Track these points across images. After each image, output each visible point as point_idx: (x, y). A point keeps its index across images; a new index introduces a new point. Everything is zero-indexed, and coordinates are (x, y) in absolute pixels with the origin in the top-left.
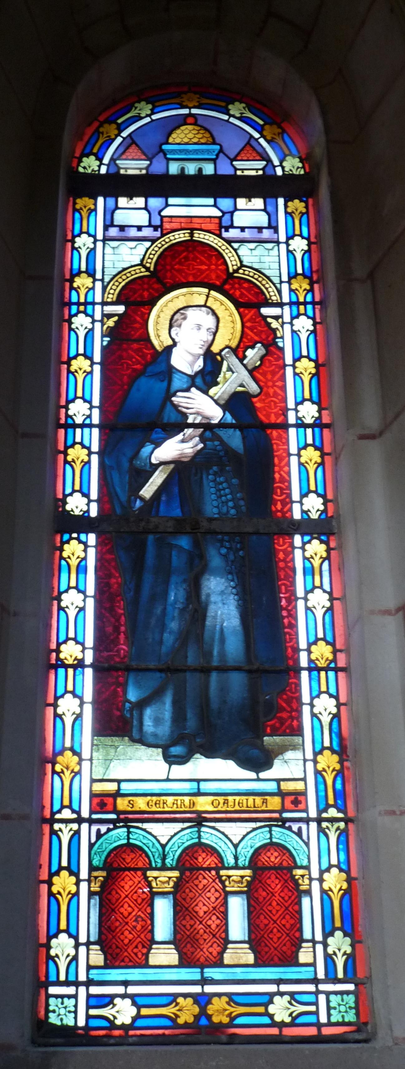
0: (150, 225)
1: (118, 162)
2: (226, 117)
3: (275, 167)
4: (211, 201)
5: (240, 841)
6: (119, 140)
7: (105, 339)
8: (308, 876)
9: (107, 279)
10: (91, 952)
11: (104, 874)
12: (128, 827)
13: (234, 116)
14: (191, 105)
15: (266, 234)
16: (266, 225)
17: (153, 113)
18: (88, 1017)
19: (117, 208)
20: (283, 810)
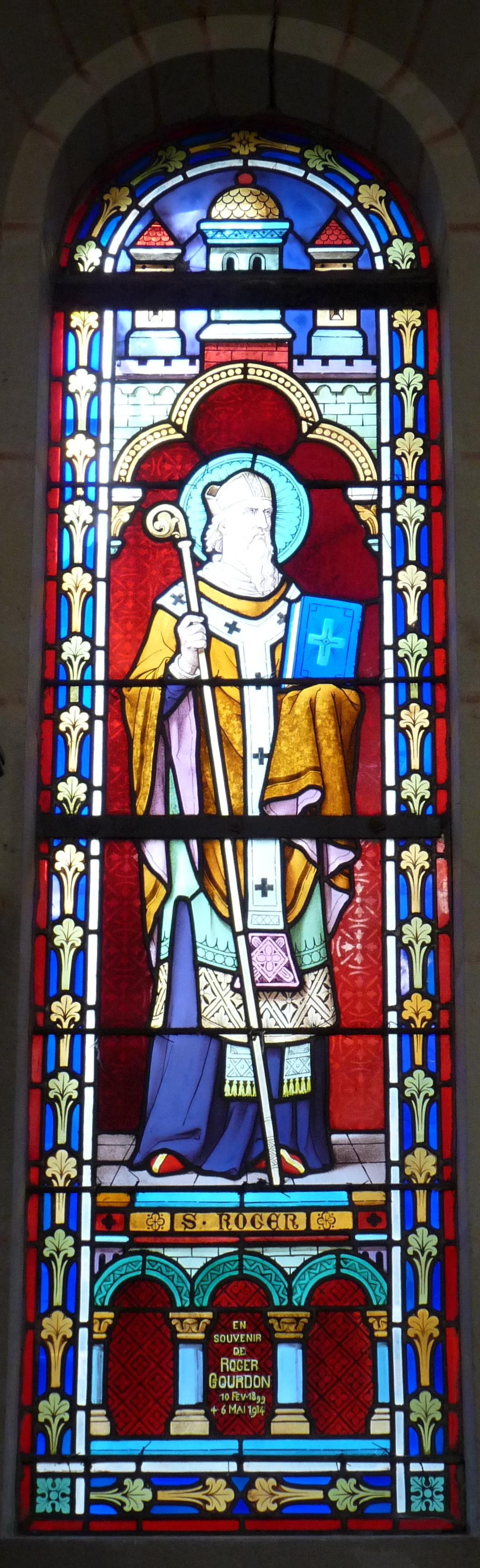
1: (133, 251)
2: (300, 173)
3: (372, 255)
5: (296, 1273)
7: (114, 543)
9: (118, 446)
10: (92, 1419)
11: (111, 1315)
12: (145, 1254)
13: (315, 172)
16: (359, 352)
18: (88, 1502)
19: (134, 329)
20: (357, 1229)
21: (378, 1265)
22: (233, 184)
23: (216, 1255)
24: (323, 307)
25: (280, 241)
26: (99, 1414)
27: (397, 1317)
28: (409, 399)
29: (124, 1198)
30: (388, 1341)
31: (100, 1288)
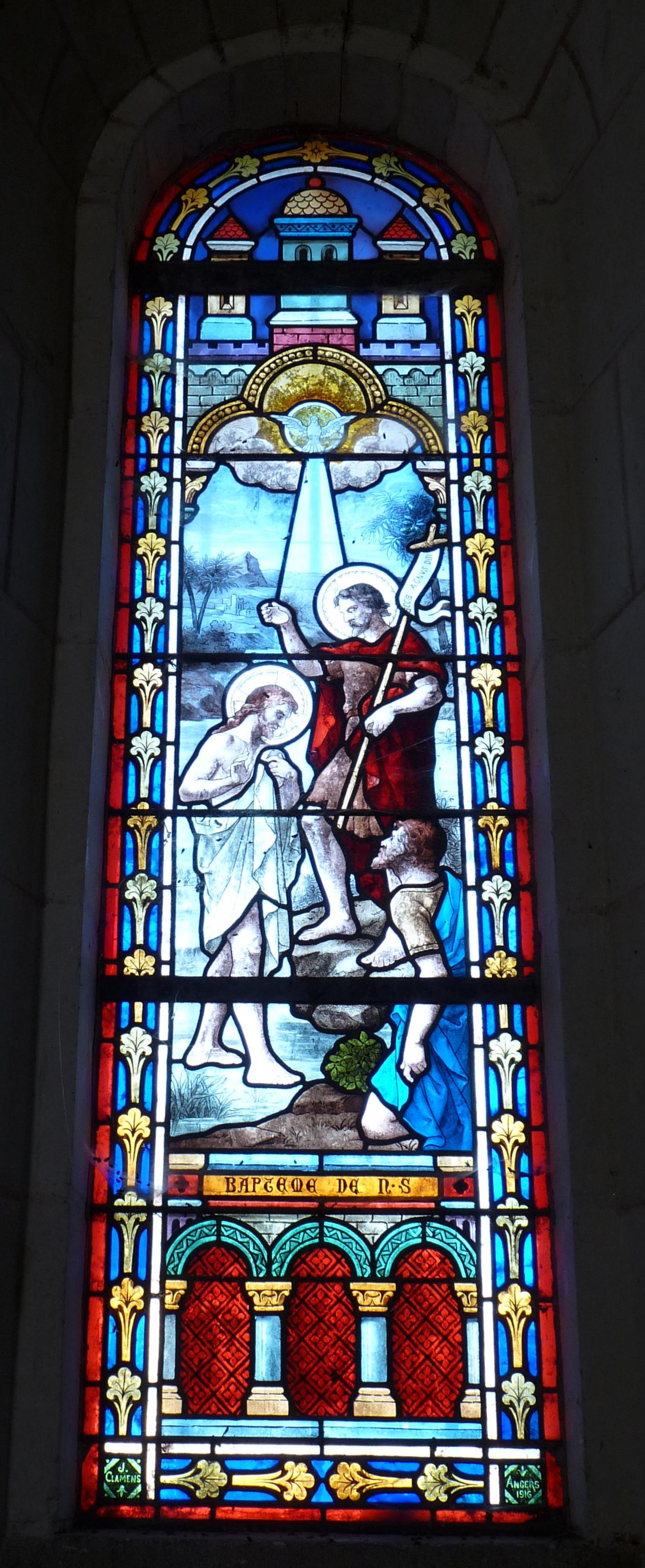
2: (368, 178)
6: (211, 211)
8: (475, 1294)
9: (191, 422)
10: (164, 1396)
13: (380, 176)
15: (428, 351)
18: (159, 1486)
20: (442, 1197)
21: (465, 1233)
22: (304, 186)
23: (295, 1221)
25: (350, 234)
26: (169, 1390)
27: (487, 1292)
31: (172, 1255)
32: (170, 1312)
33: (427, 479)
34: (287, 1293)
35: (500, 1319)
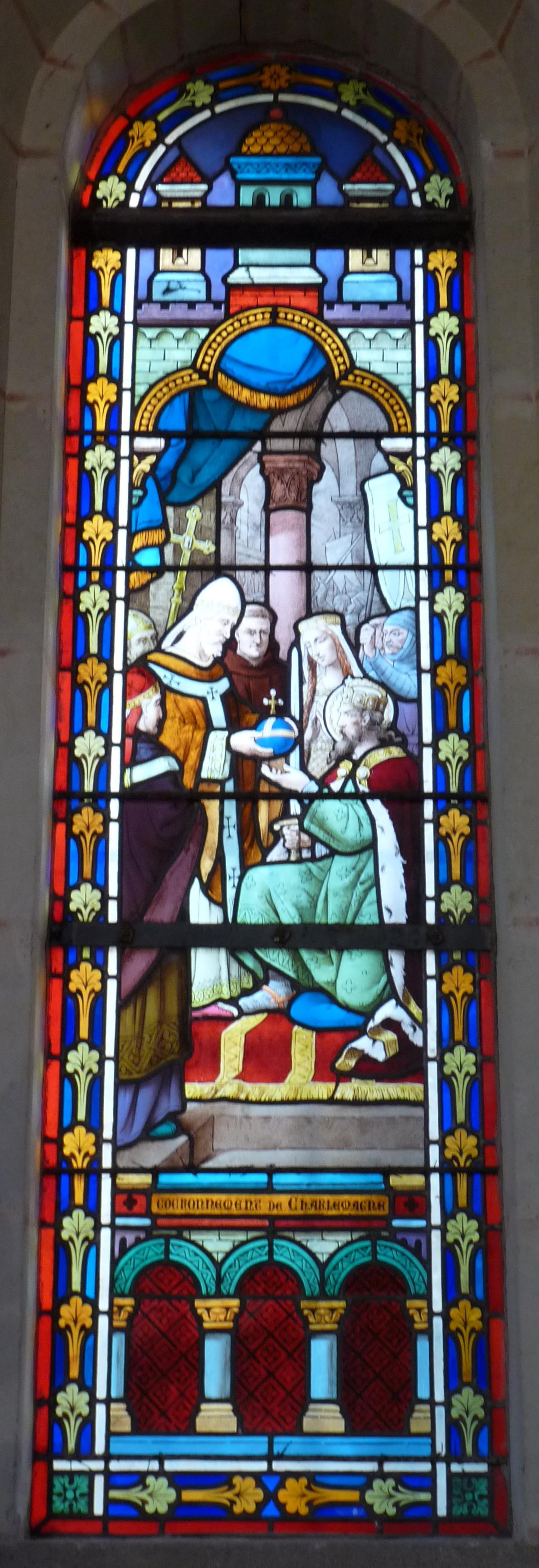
0: (209, 299)
2: (332, 107)
4: (304, 255)
8: (426, 1311)
14: (274, 86)
17: (217, 99)
24: (356, 246)
26: (119, 1410)
28: (444, 345)
29: (147, 1179)
30: (429, 1332)
32: (119, 1329)
33: (392, 459)
34: (236, 1310)
35: (450, 1337)
